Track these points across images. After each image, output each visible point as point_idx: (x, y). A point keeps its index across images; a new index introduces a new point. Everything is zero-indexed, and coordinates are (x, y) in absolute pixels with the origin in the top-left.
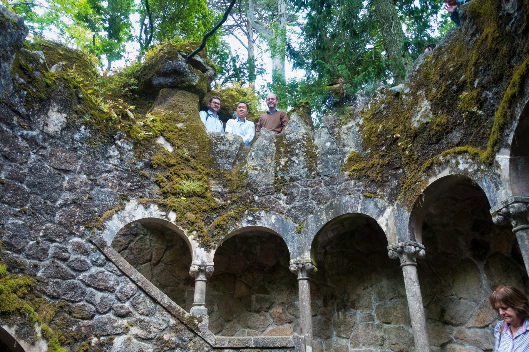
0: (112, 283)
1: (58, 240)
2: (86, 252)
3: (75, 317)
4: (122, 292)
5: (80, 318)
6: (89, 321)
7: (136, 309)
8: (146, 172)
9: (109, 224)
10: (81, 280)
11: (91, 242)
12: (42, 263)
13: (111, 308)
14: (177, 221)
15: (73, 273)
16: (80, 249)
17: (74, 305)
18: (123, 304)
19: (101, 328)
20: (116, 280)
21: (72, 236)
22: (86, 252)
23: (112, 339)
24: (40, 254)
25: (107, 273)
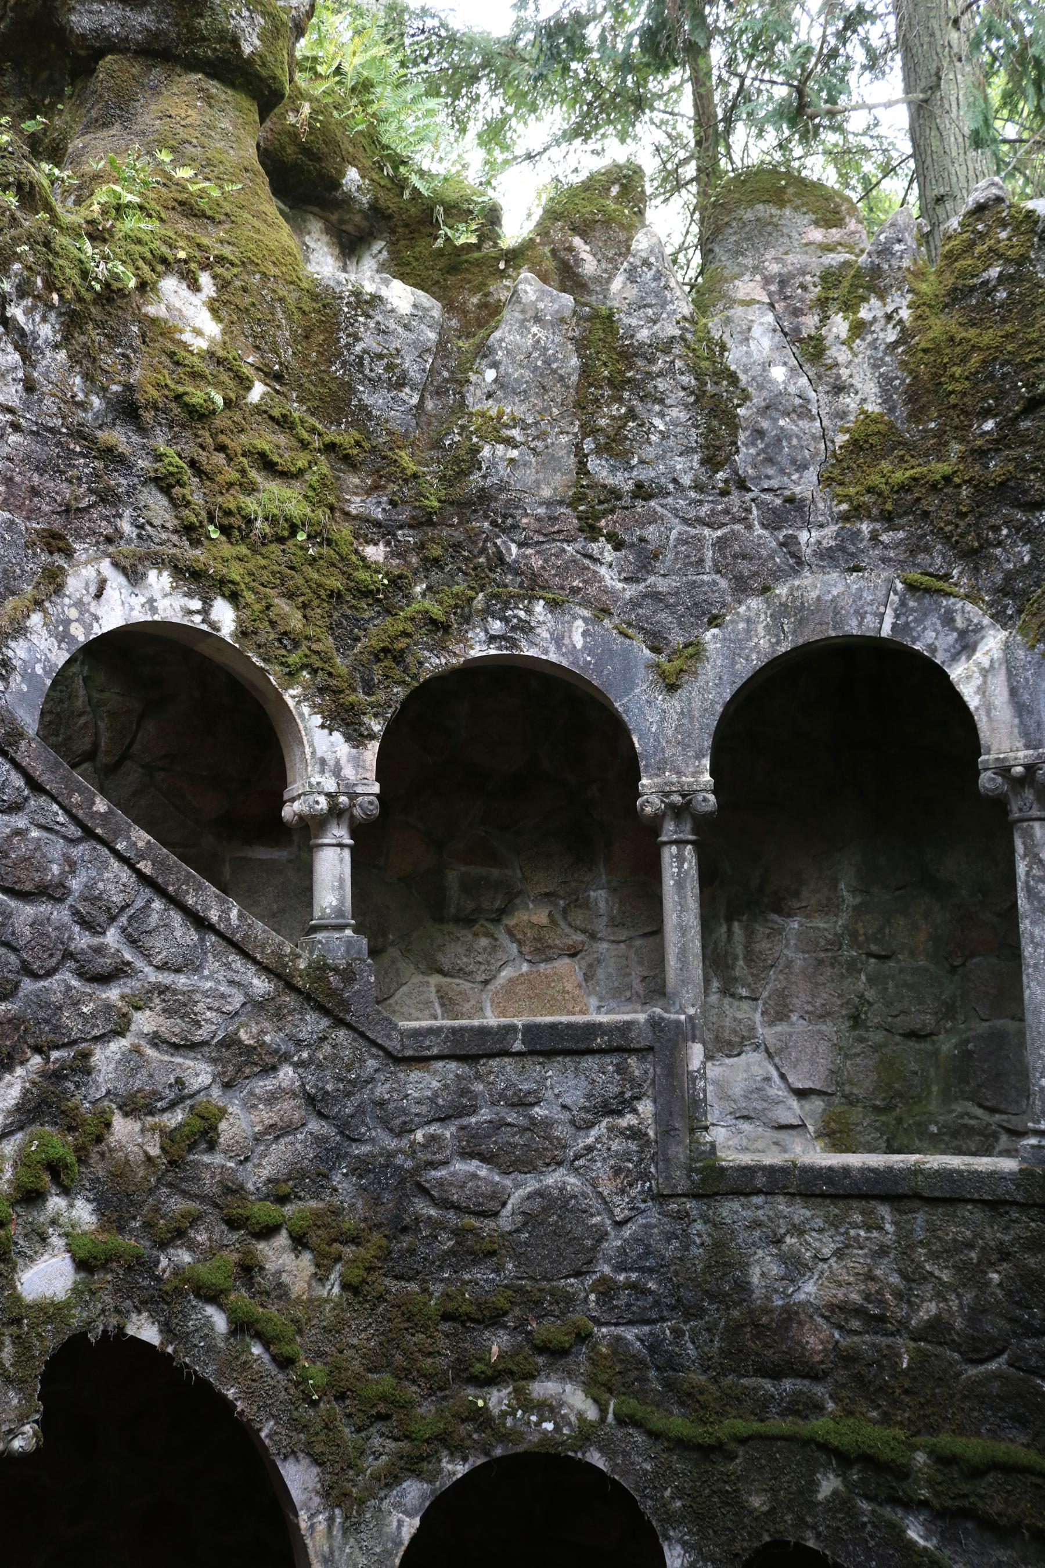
4: (93, 898)
7: (147, 956)
13: (68, 955)
14: (243, 633)
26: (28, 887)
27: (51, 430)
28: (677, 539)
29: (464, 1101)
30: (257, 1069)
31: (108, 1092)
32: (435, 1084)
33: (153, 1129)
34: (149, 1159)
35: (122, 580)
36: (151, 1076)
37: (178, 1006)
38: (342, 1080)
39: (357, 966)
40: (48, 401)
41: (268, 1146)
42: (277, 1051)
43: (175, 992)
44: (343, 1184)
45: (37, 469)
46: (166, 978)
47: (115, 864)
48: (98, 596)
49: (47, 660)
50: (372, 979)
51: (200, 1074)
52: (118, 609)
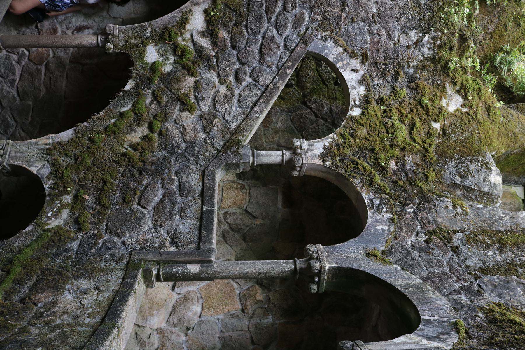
0: (269, 59)
2: (296, 28)
3: (232, 29)
4: (260, 71)
6: (230, 44)
8: (402, 78)
9: (330, 43)
10: (268, 29)
11: (307, 29)
15: (273, 19)
17: (243, 28)
18: (248, 75)
19: (224, 57)
20: (272, 64)
21: (309, 11)
22: (296, 26)
25: (279, 53)
26: (263, 50)
27: (398, 55)
28: (439, 259)
29: (186, 192)
30: (205, 125)
31: (202, 77)
32: (193, 183)
33: (190, 91)
34: (180, 89)
35: (359, 78)
36: (206, 90)
37: (227, 99)
38: (199, 153)
39: (239, 157)
40: (406, 53)
41: (178, 129)
42: (210, 131)
43: (232, 98)
44: (162, 153)
45: (385, 51)
46: (236, 96)
47: (271, 78)
48: (352, 70)
50: (234, 162)
51: (205, 107)
52: (350, 78)
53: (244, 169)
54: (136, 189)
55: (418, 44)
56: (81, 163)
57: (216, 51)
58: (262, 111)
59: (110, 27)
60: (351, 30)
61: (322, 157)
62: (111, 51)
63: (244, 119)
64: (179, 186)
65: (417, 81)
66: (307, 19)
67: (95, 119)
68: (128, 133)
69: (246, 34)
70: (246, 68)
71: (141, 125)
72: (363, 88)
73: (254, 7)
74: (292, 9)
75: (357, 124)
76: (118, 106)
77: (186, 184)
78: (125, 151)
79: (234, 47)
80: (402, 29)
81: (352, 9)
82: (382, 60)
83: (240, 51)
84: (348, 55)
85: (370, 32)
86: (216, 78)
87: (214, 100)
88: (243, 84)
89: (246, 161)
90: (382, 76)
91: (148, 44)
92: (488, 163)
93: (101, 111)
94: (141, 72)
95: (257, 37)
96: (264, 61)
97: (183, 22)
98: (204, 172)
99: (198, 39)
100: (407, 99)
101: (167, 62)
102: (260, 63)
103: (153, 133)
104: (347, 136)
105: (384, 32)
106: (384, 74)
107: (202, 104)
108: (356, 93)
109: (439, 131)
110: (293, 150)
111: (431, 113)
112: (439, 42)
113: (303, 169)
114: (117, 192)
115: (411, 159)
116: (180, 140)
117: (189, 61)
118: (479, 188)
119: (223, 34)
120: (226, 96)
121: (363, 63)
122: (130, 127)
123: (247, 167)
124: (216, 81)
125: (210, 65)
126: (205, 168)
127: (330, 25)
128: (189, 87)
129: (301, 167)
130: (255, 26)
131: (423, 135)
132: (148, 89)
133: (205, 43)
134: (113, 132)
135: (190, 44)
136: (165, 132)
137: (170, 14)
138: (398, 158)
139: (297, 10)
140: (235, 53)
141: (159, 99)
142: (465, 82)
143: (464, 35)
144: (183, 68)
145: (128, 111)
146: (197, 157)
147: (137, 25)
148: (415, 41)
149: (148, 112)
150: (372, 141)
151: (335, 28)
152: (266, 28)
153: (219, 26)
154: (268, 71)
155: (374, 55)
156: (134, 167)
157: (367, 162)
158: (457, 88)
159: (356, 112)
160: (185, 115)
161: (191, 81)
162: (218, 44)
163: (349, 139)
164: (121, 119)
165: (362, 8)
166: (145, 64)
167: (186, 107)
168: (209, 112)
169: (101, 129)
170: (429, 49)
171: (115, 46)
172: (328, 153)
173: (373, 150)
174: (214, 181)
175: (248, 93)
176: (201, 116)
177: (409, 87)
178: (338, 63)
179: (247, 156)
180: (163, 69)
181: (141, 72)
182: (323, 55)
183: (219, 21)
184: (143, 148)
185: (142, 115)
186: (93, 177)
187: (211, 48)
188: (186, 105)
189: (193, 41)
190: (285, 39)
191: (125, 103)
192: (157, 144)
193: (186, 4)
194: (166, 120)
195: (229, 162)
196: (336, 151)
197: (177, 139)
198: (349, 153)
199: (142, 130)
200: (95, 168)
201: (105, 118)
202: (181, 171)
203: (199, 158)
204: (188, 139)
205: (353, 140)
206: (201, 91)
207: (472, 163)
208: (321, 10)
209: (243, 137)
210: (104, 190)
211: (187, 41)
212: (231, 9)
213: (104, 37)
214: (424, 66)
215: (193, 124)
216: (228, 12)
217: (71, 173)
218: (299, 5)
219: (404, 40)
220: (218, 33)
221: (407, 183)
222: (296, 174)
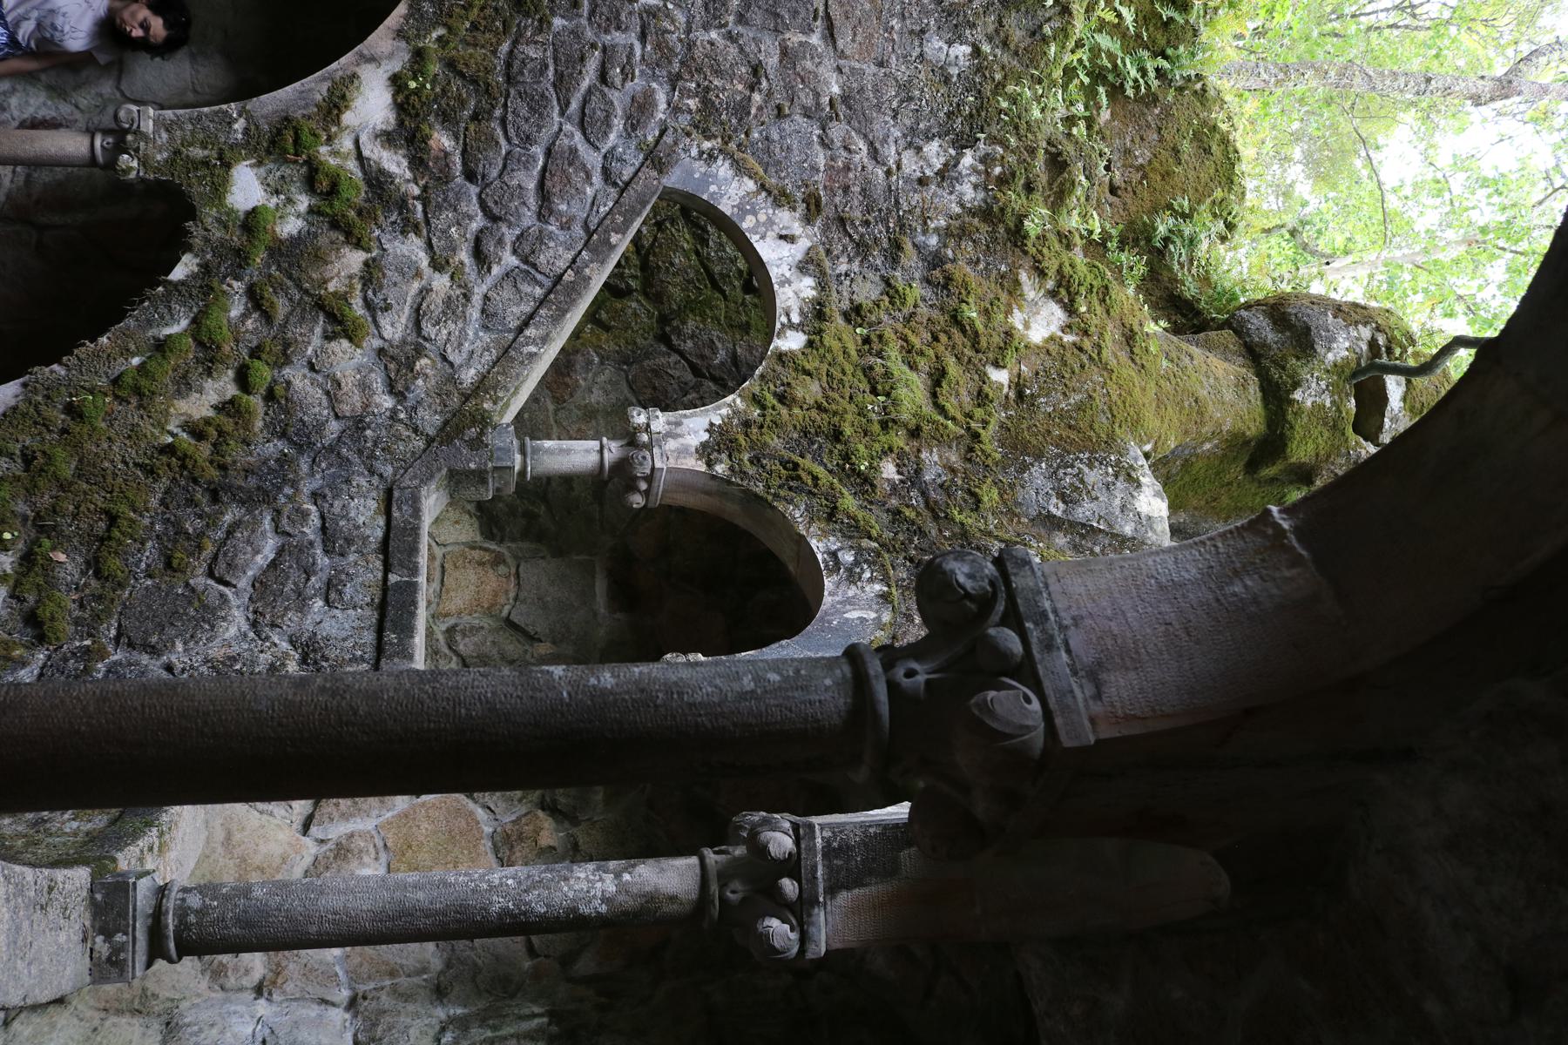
0: (563, 207)
1: (649, 48)
2: (634, 130)
3: (466, 129)
4: (540, 238)
5: (465, 144)
6: (459, 167)
8: (910, 258)
9: (723, 169)
11: (663, 132)
12: (584, 22)
15: (574, 105)
16: (641, 108)
17: (495, 125)
18: (508, 247)
19: (445, 200)
20: (571, 219)
21: (667, 87)
22: (633, 125)
23: (418, 233)
24: (604, 9)
26: (548, 184)
30: (393, 375)
32: (361, 520)
35: (799, 256)
36: (395, 284)
38: (375, 444)
41: (320, 386)
42: (407, 389)
44: (274, 447)
46: (477, 300)
47: (569, 256)
48: (781, 237)
49: (722, 196)
51: (394, 327)
52: (777, 257)
53: (498, 490)
54: (201, 535)
55: (947, 174)
56: (42, 470)
57: (421, 183)
58: (545, 340)
59: (130, 111)
60: (776, 136)
61: (704, 451)
62: (133, 175)
63: (498, 359)
64: (324, 529)
65: (948, 266)
66: (662, 106)
67: (83, 356)
68: (179, 394)
69: (503, 142)
70: (504, 229)
71: (215, 374)
72: (809, 281)
73: (522, 74)
74: (624, 80)
75: (796, 370)
76: (150, 323)
77: (342, 523)
78: (170, 440)
79: (470, 176)
80: (905, 136)
81: (778, 85)
82: (857, 214)
83: (488, 185)
84: (770, 200)
85: (825, 143)
86: (422, 254)
87: (418, 310)
88: (496, 270)
89: (504, 464)
90: (858, 254)
91: (237, 161)
92: (1131, 466)
93: (101, 334)
94: (218, 234)
95: (533, 149)
96: (551, 212)
97: (335, 105)
98: (389, 492)
99: (373, 151)
100: (923, 310)
101: (290, 209)
102: (540, 216)
103: (249, 393)
104: (771, 400)
105: (862, 145)
106: (862, 249)
107: (385, 321)
108: (791, 294)
109: (1006, 390)
110: (630, 438)
111: (983, 343)
112: (998, 170)
113: (655, 484)
114: (149, 544)
115: (936, 458)
116: (325, 412)
117: (348, 209)
118: (1110, 526)
119: (442, 140)
120: (448, 301)
121: (808, 220)
122: (184, 377)
123: (507, 484)
124: (424, 260)
125: (406, 221)
126: (394, 482)
127: (722, 123)
128: (351, 277)
129: (650, 479)
130: (527, 120)
131: (966, 399)
132: (237, 278)
133: (394, 163)
134: (137, 391)
135: (352, 164)
136: (283, 393)
137: (297, 85)
138: (901, 455)
139: (637, 84)
140: (474, 190)
141: (266, 304)
142: (1067, 270)
143: (1060, 154)
144: (334, 225)
145: (179, 335)
146: (372, 456)
147: (206, 109)
148: (938, 164)
149: (237, 341)
150: (835, 413)
151: (735, 130)
152: (556, 128)
153: (432, 118)
154: (562, 238)
155: (837, 200)
156: (195, 481)
157: (822, 463)
158: (1050, 284)
159: (792, 342)
160: (337, 350)
161: (354, 259)
162: (427, 166)
163: (773, 408)
164: (158, 355)
165: (803, 81)
166: (228, 214)
167: (340, 326)
168: (404, 342)
169: (102, 382)
170: (975, 187)
171: (144, 163)
172: (720, 442)
173: (837, 435)
174: (417, 513)
175: (507, 292)
176: (381, 352)
177: (927, 281)
178: (743, 219)
179: (507, 451)
180: (278, 229)
181: (218, 234)
182: (705, 197)
183: (430, 107)
184: (221, 433)
185: (219, 347)
186: (77, 507)
187: (408, 175)
188: (340, 323)
189: (360, 157)
190: (605, 157)
191: (172, 316)
192: (259, 424)
193: (343, 60)
194: (288, 361)
195: (459, 466)
196: (741, 438)
197: (317, 410)
198: (775, 442)
199: (221, 387)
200: (85, 486)
201: (114, 352)
202: (327, 491)
203: (377, 459)
204: (345, 409)
205: (784, 411)
206: (381, 287)
207: (1091, 466)
208: (698, 85)
209: (495, 403)
210: (110, 538)
211: (346, 157)
212: (462, 75)
213: (110, 140)
214: (962, 228)
215: (359, 372)
216: (456, 85)
217: (13, 498)
218: (642, 72)
219: (911, 165)
220: (429, 137)
221: (926, 513)
222: (637, 501)
